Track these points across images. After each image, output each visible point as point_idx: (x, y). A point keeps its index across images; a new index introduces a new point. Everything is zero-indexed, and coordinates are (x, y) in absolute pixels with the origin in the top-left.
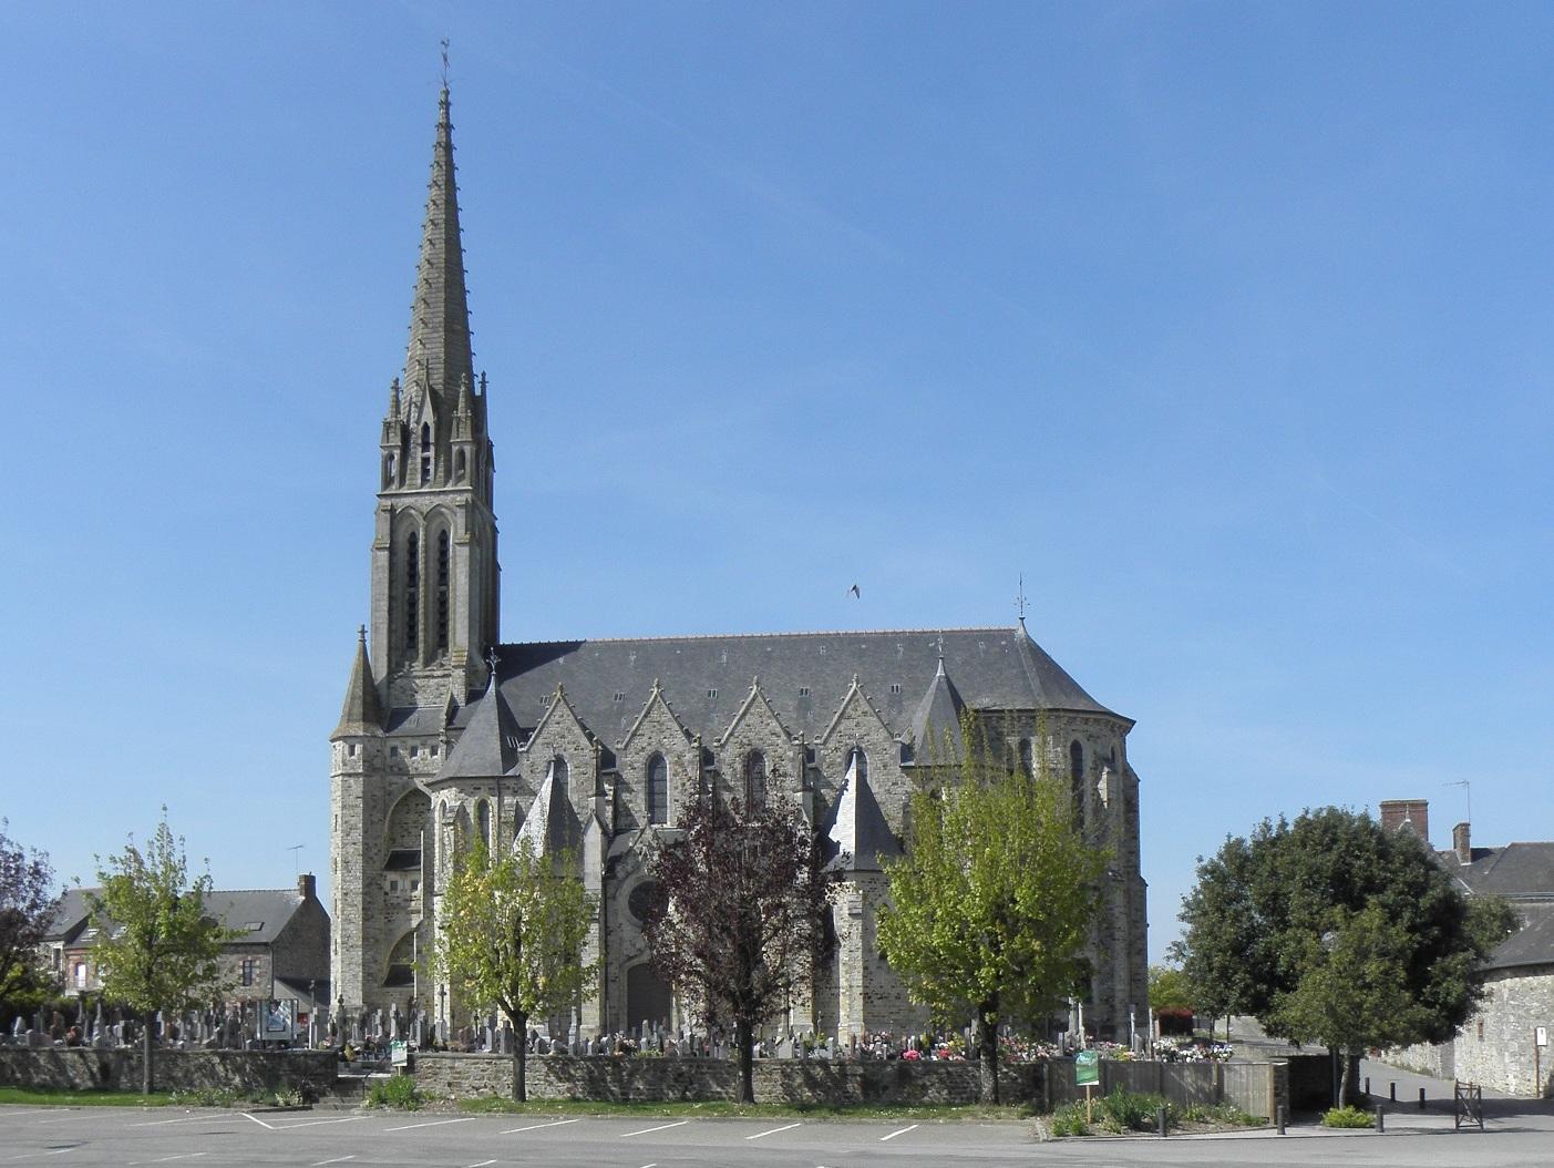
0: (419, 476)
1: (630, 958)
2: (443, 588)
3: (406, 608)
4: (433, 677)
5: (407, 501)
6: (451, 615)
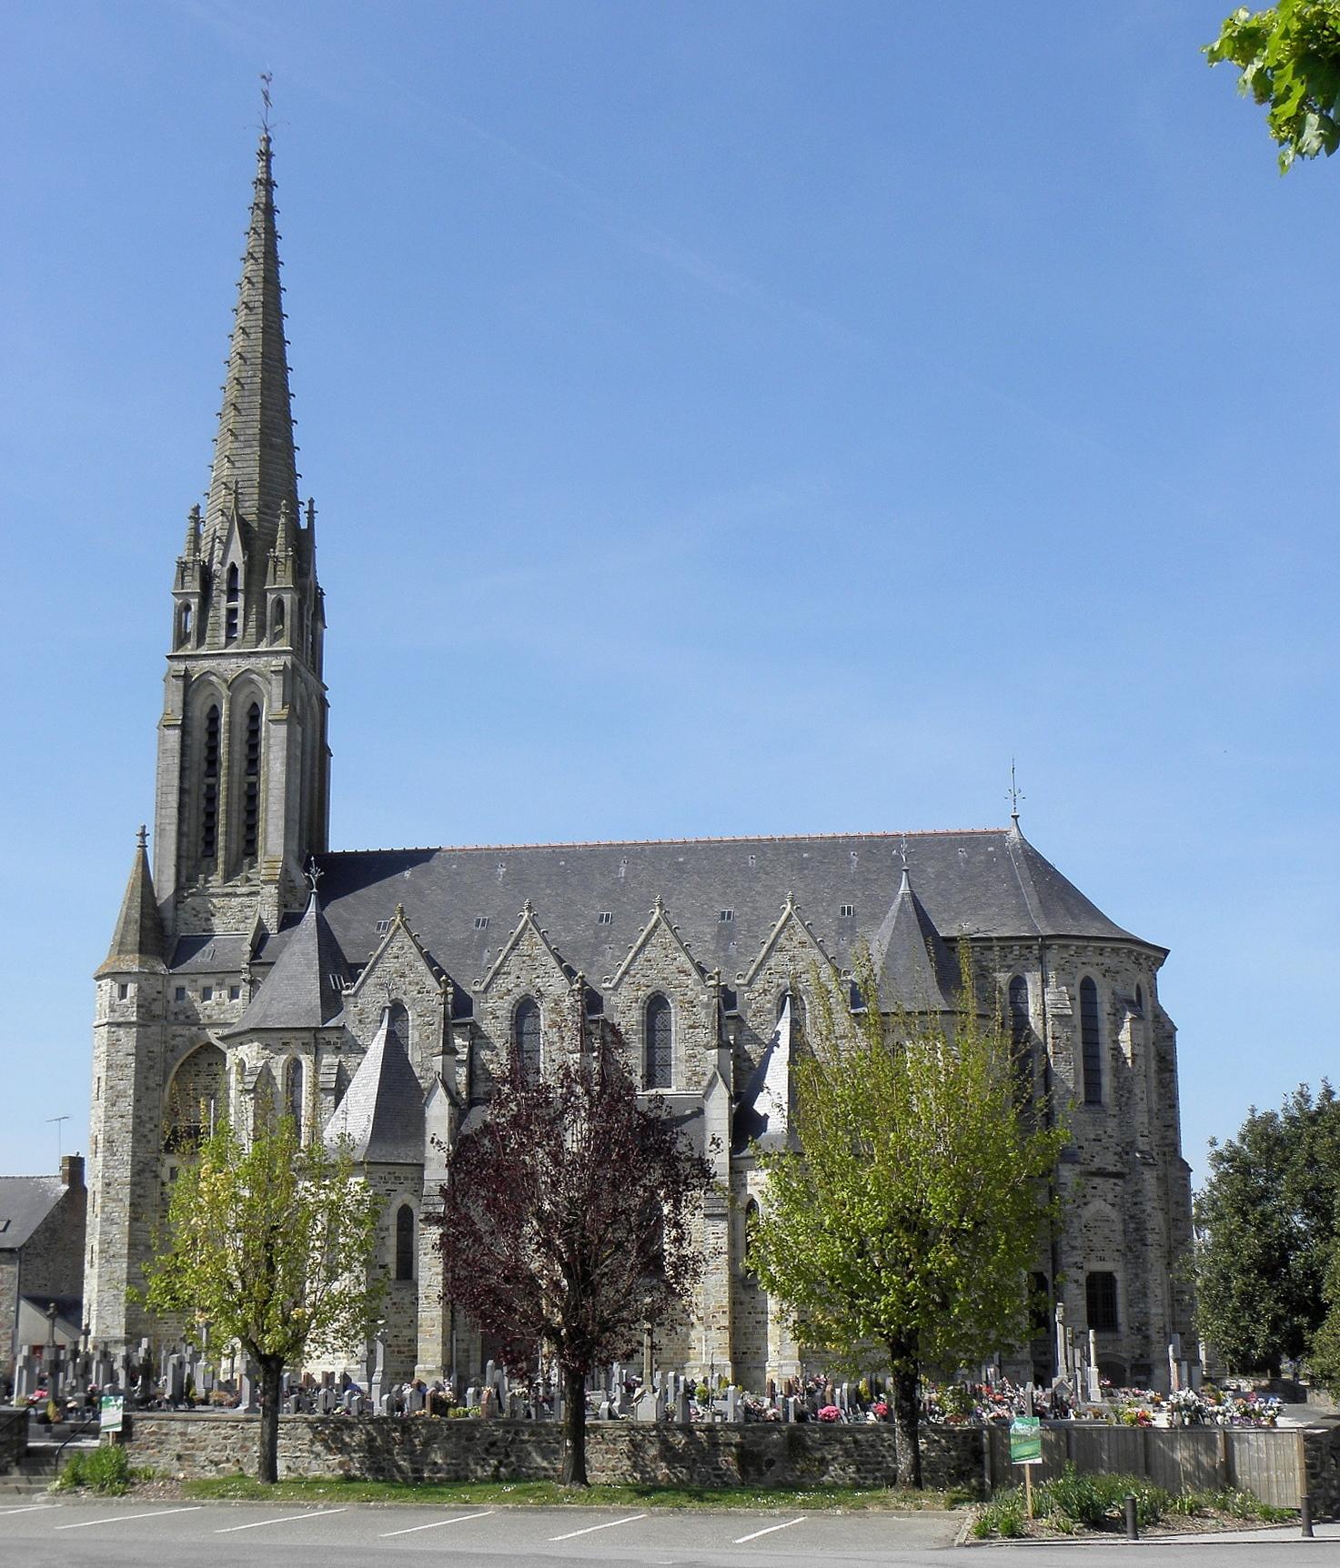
0: (223, 633)
2: (252, 779)
3: (203, 803)
4: (236, 895)
5: (206, 665)
6: (262, 815)
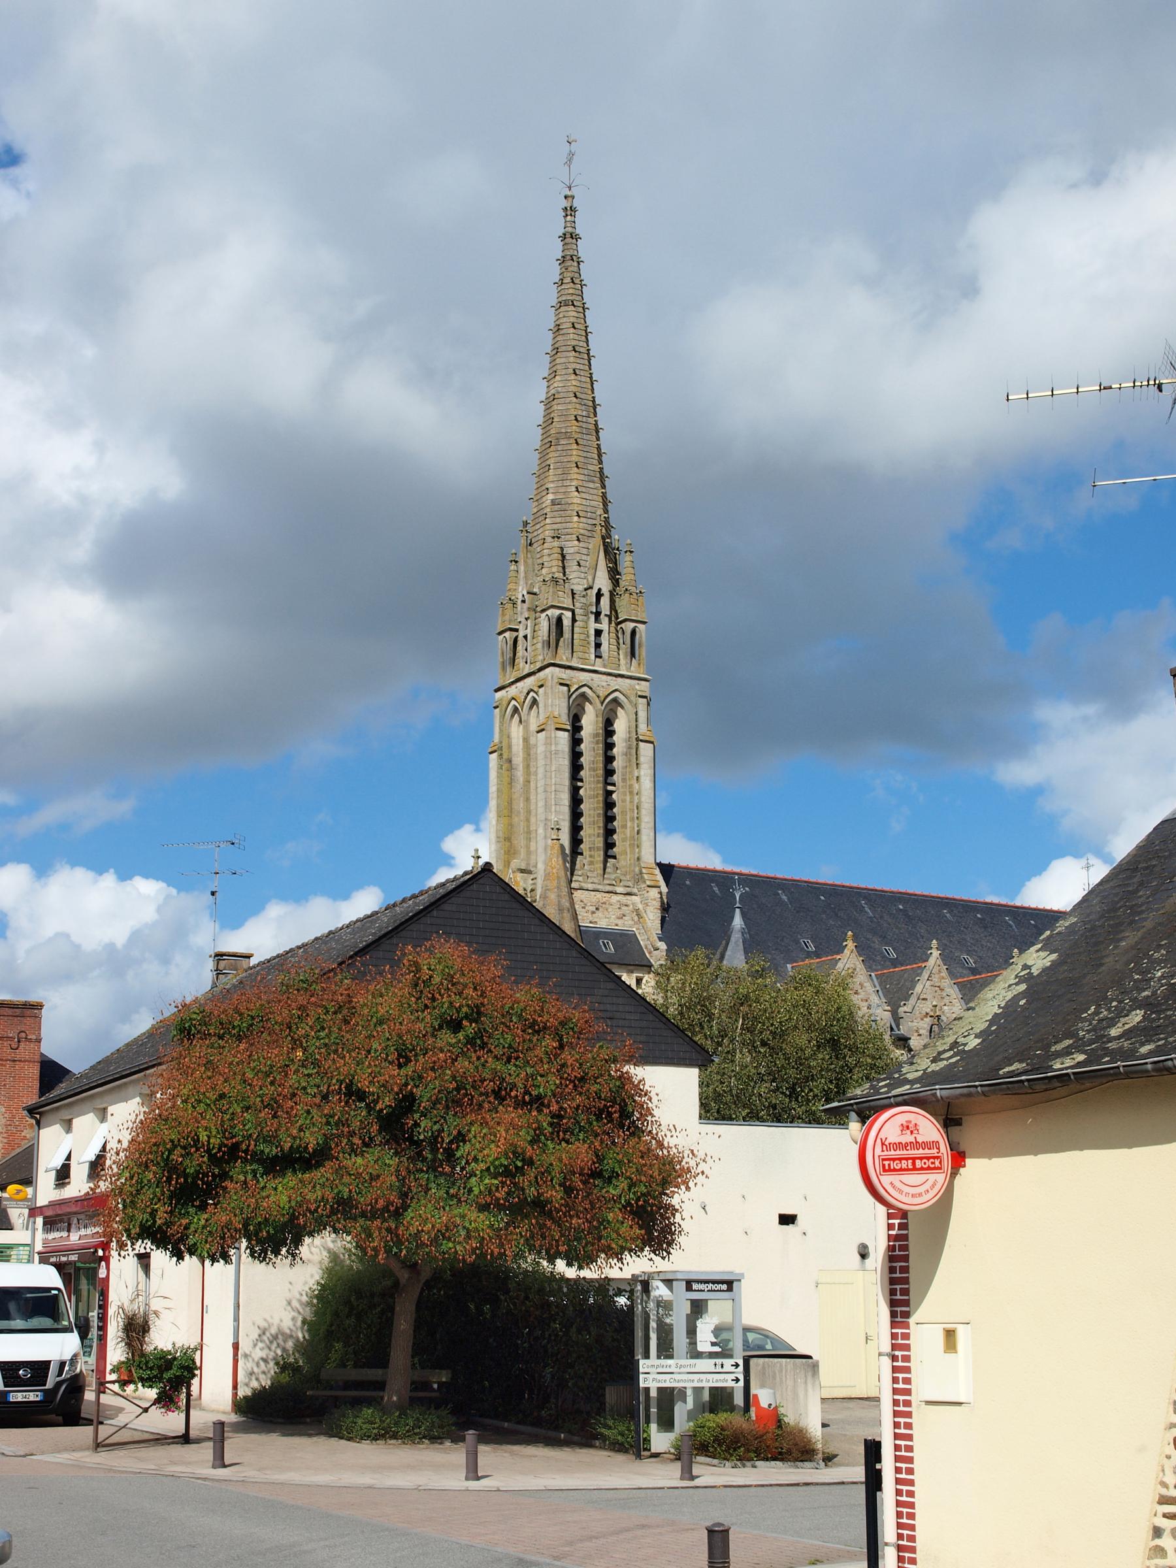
0: (593, 650)
5: (584, 677)
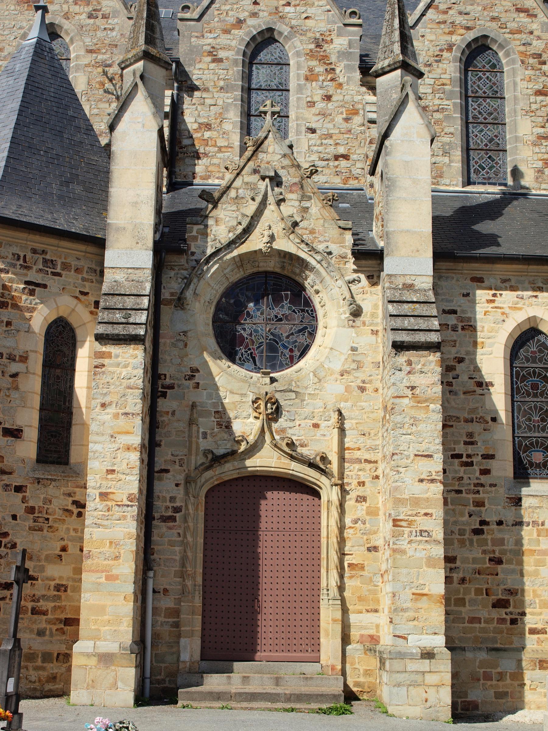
1: (217, 460)
